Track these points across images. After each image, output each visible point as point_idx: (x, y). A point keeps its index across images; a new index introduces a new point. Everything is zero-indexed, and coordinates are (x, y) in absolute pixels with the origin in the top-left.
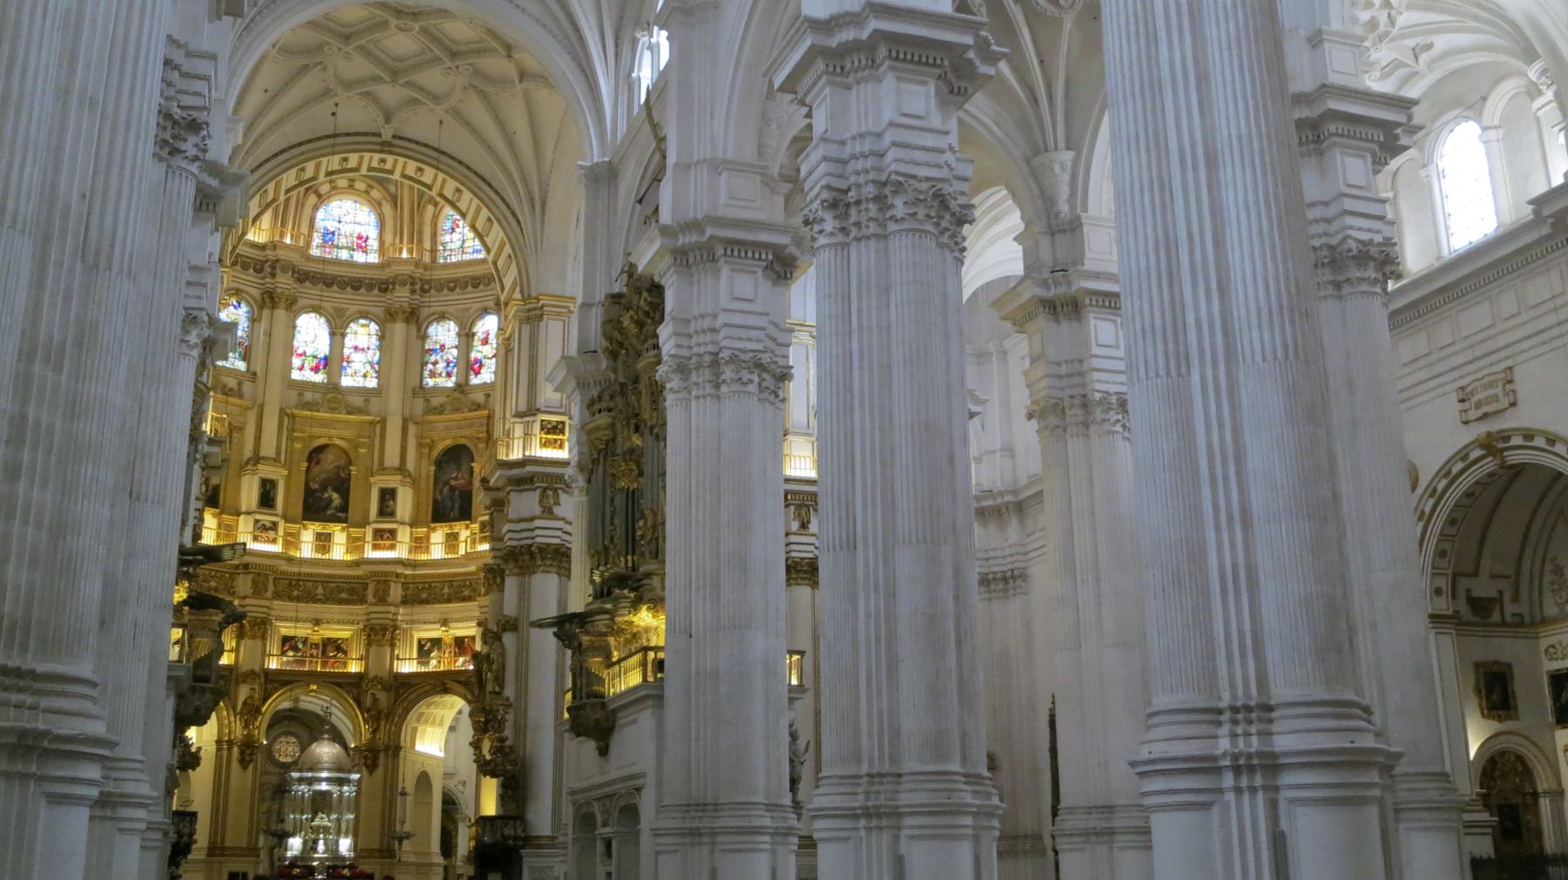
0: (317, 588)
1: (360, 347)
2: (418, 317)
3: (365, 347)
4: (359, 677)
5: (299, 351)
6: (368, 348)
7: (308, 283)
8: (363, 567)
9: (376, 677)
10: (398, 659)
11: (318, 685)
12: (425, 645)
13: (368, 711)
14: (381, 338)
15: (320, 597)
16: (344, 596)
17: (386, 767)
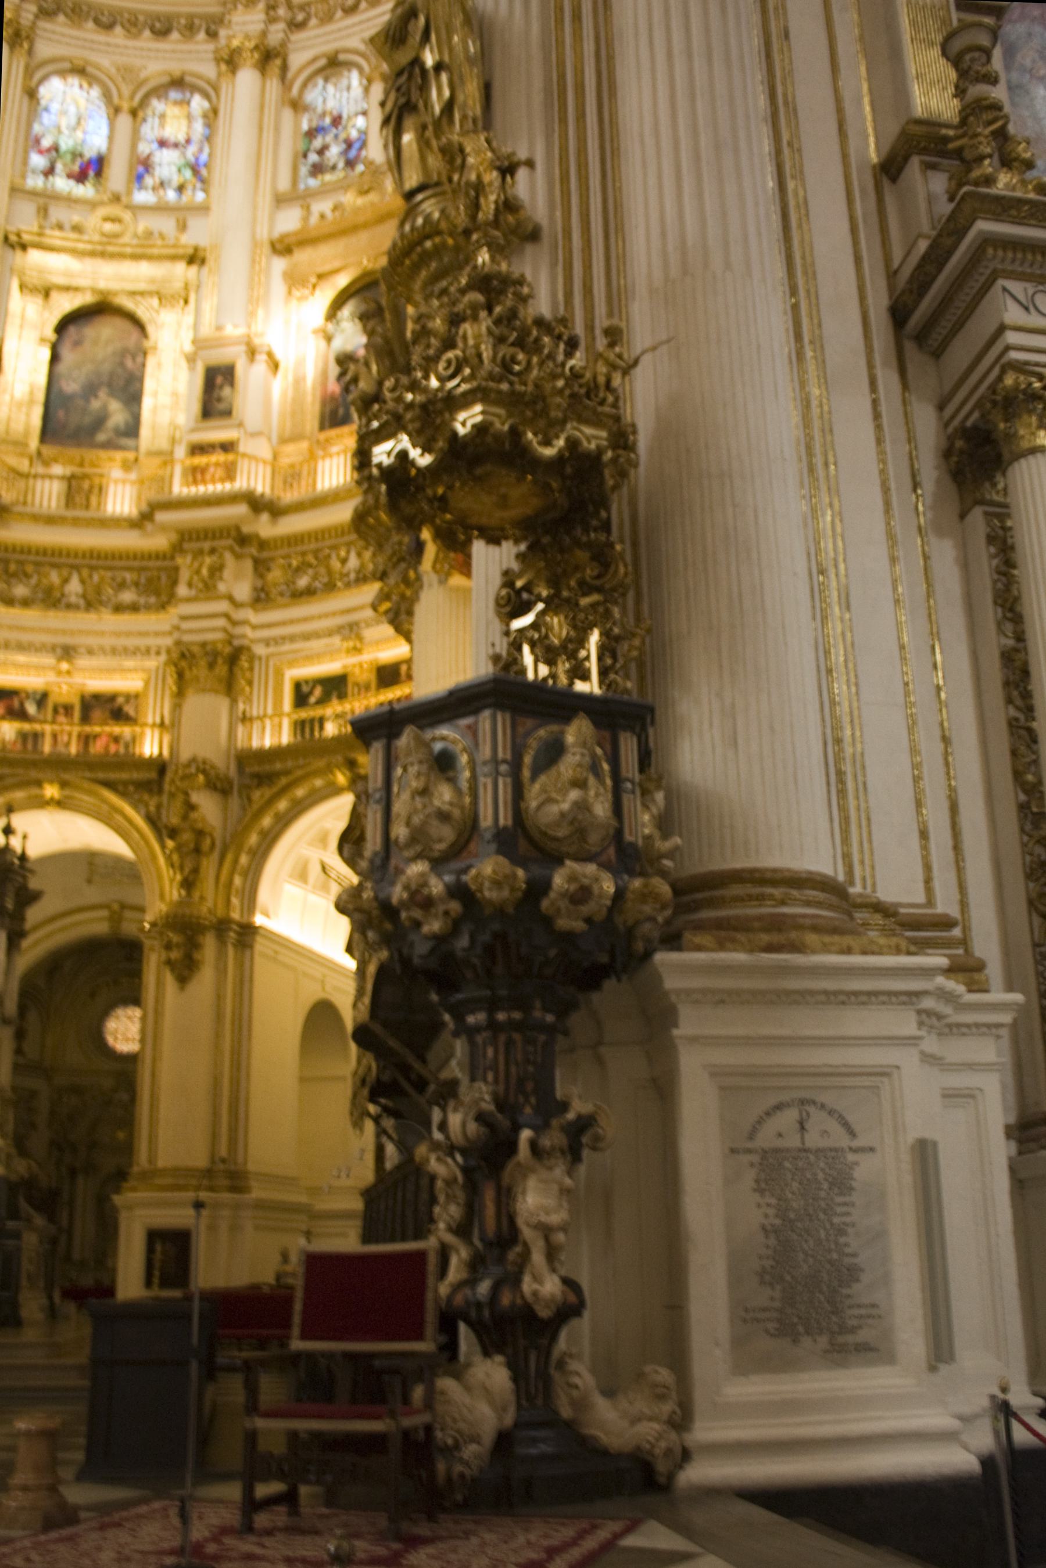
0: (66, 581)
1: (172, 139)
2: (284, 68)
3: (181, 138)
4: (160, 766)
5: (46, 143)
6: (188, 141)
7: (61, 18)
8: (161, 517)
9: (194, 760)
10: (245, 719)
11: (64, 785)
12: (311, 693)
13: (173, 833)
14: (212, 116)
15: (73, 599)
16: (128, 596)
17: (221, 971)
